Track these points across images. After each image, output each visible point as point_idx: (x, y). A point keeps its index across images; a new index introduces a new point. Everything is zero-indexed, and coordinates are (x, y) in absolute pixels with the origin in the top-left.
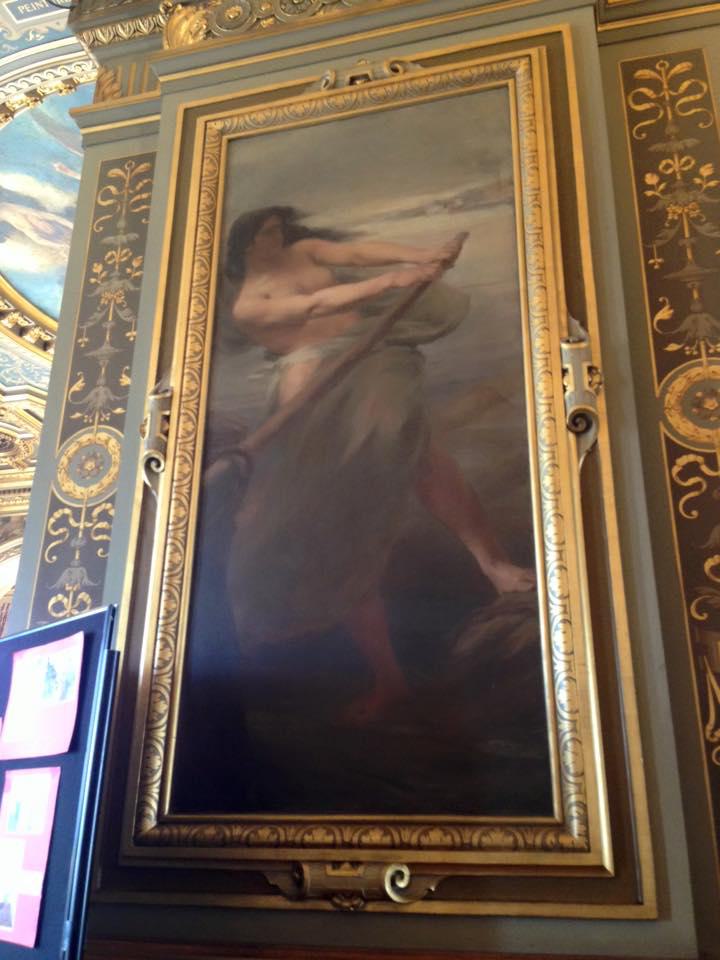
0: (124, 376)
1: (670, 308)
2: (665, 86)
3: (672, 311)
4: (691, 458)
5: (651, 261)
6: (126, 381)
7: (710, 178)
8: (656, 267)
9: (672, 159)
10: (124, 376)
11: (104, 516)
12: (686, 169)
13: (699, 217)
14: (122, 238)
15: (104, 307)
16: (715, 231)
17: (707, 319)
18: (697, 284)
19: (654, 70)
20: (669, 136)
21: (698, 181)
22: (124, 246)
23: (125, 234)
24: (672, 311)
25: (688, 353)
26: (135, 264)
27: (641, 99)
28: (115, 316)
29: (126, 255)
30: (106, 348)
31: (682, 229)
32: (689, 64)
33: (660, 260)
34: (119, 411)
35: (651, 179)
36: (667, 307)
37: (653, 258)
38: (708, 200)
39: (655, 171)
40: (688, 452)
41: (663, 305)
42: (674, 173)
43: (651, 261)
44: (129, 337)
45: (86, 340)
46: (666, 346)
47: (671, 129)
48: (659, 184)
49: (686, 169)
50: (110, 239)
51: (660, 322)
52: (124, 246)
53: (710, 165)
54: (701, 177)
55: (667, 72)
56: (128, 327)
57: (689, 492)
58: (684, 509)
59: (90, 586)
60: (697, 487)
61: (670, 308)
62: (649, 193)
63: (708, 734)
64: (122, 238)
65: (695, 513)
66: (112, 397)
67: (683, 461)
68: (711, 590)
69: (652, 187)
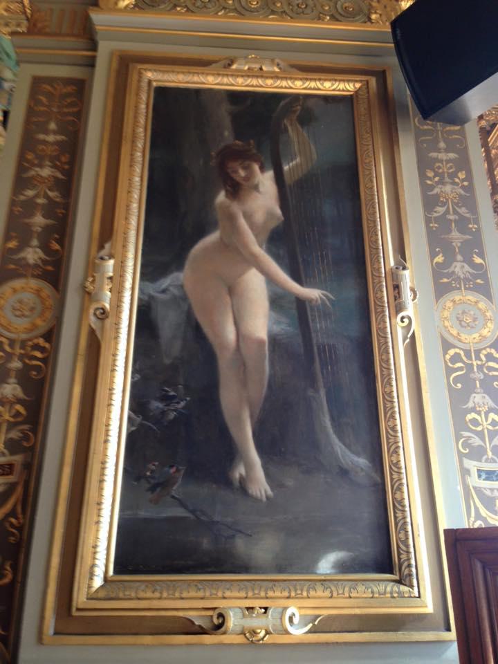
3: (443, 258)
4: (457, 350)
7: (463, 180)
8: (434, 229)
12: (451, 171)
13: (458, 203)
14: (51, 138)
16: (468, 213)
18: (459, 244)
20: (440, 149)
21: (457, 180)
24: (443, 258)
25: (454, 285)
31: (448, 208)
33: (436, 225)
36: (441, 255)
38: (462, 192)
39: (433, 170)
40: (455, 347)
42: (443, 172)
43: (431, 225)
45: (21, 210)
48: (434, 177)
49: (451, 171)
54: (459, 178)
57: (457, 371)
59: (25, 400)
60: (460, 369)
62: (429, 182)
63: (471, 522)
65: (459, 385)
67: (452, 352)
69: (430, 179)
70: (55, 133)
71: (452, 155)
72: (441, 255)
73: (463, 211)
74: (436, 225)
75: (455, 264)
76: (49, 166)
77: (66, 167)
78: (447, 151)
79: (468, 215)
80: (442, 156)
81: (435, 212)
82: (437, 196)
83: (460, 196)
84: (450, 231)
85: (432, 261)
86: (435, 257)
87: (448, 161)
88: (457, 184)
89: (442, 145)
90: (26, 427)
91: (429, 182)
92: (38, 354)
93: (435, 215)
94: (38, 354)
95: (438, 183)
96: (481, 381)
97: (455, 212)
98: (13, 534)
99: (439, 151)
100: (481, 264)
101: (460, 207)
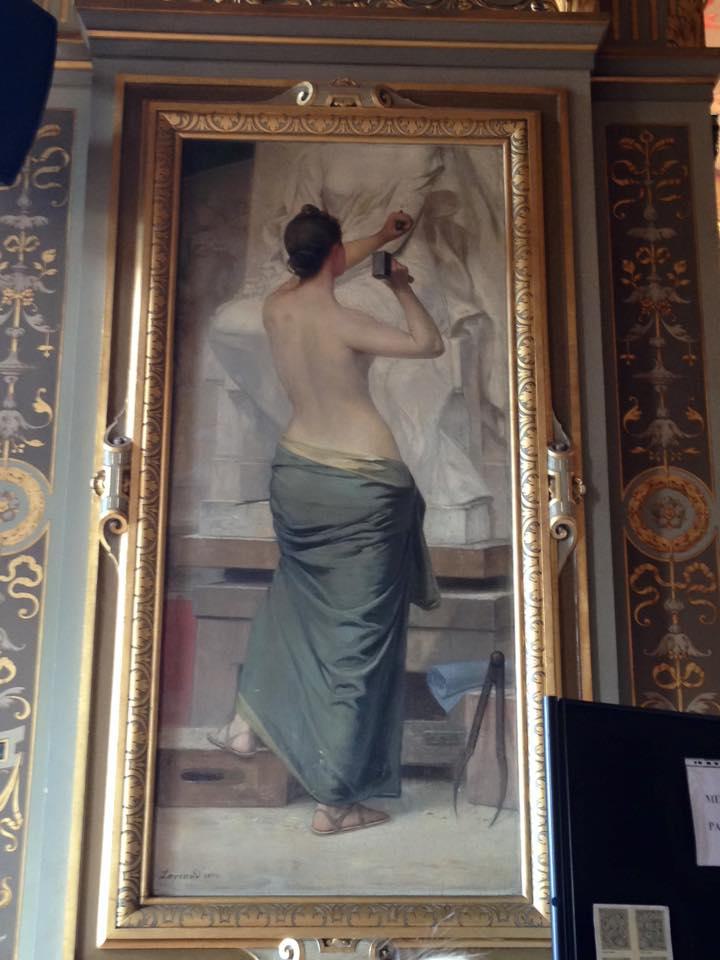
0: (39, 400)
1: (638, 410)
3: (640, 413)
5: (624, 357)
6: (41, 407)
9: (650, 248)
10: (39, 400)
11: (23, 570)
15: (7, 308)
16: (683, 334)
17: (670, 426)
22: (29, 232)
23: (29, 215)
24: (640, 413)
25: (651, 458)
26: (48, 256)
27: (623, 172)
28: (23, 323)
30: (12, 361)
33: (632, 357)
34: (36, 443)
35: (629, 267)
37: (626, 353)
41: (630, 405)
43: (624, 357)
46: (633, 448)
47: (649, 212)
50: (10, 219)
51: (630, 422)
52: (29, 232)
53: (682, 262)
54: (674, 273)
56: (40, 338)
58: (639, 616)
61: (638, 410)
64: (26, 221)
66: (24, 424)
68: (657, 694)
69: (628, 276)
71: (667, 232)
73: (675, 330)
74: (632, 357)
75: (658, 422)
77: (51, 272)
78: (658, 224)
79: (683, 339)
80: (652, 234)
81: (633, 334)
83: (675, 305)
84: (650, 367)
86: (626, 413)
87: (659, 243)
88: (671, 283)
90: (17, 690)
91: (626, 281)
92: (27, 582)
94: (27, 582)
95: (639, 283)
96: (680, 614)
97: (664, 333)
98: (8, 841)
100: (698, 421)
101: (672, 325)
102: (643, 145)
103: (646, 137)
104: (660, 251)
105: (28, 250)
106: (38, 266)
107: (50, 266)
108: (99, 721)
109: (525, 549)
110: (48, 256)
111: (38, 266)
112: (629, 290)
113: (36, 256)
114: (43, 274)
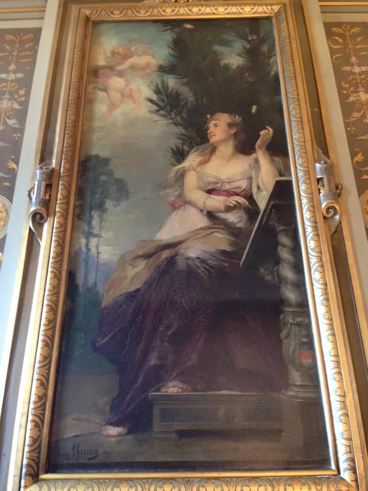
1: (362, 156)
2: (348, 38)
3: (363, 157)
5: (349, 129)
14: (12, 76)
19: (342, 29)
24: (363, 157)
26: (22, 92)
29: (14, 86)
32: (360, 29)
33: (354, 129)
44: (15, 137)
50: (3, 76)
51: (357, 162)
55: (349, 31)
61: (362, 156)
64: (12, 76)
69: (346, 89)
70: (15, 72)
72: (360, 154)
74: (354, 129)
76: (8, 99)
77: (23, 99)
78: (359, 65)
81: (353, 117)
82: (354, 102)
85: (352, 160)
89: (354, 59)
91: (345, 92)
93: (353, 119)
99: (352, 65)
102: (344, 31)
103: (345, 27)
104: (362, 77)
105: (12, 89)
106: (16, 96)
107: (23, 96)
108: (19, 346)
109: (306, 222)
110: (22, 92)
111: (16, 96)
112: (348, 96)
113: (17, 92)
114: (19, 100)
